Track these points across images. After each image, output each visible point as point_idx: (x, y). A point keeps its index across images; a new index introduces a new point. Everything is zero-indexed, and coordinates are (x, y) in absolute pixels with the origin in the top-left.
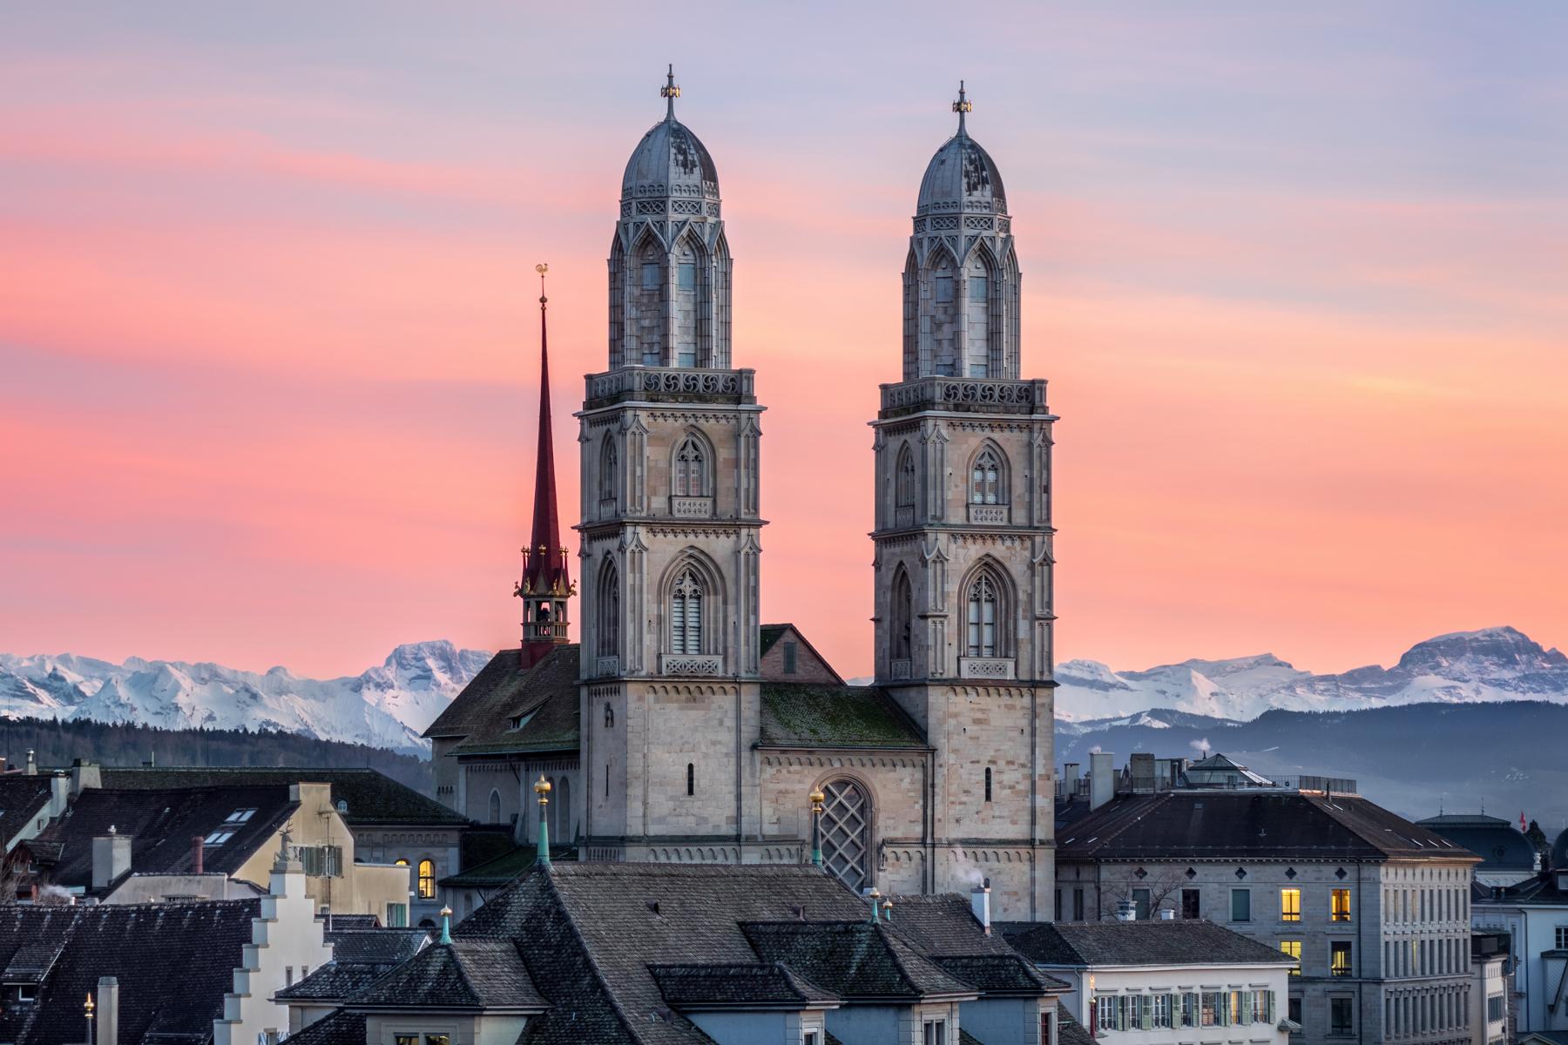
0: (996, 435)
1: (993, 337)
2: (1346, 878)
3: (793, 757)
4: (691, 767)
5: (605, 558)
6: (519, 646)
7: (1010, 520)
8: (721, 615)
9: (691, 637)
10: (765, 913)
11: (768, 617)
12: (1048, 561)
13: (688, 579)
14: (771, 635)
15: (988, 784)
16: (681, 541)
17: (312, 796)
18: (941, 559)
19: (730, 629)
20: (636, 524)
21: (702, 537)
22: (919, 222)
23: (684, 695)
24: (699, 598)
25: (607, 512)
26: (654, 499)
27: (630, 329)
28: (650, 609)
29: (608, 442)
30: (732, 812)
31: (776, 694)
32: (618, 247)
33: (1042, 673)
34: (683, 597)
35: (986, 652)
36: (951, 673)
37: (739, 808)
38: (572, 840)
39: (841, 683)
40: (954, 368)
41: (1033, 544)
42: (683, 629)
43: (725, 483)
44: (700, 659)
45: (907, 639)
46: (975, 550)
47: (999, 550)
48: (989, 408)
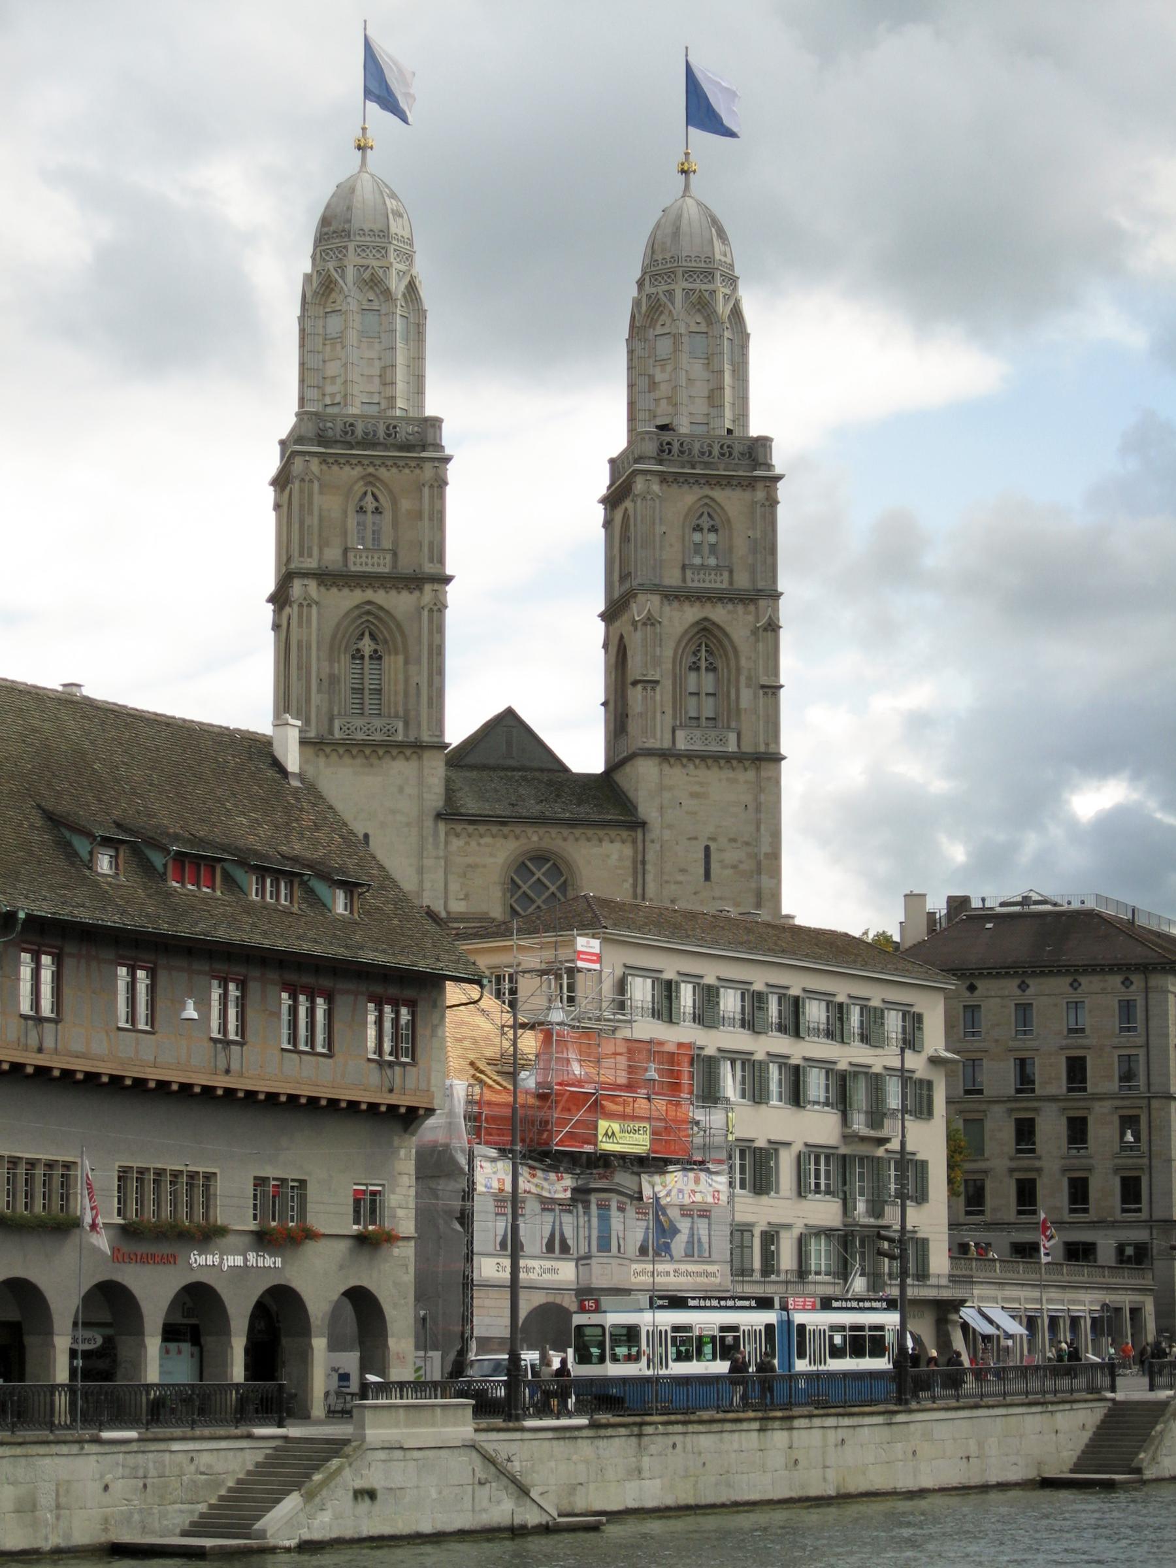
0: (718, 494)
2: (1133, 988)
3: (482, 829)
7: (731, 583)
8: (401, 677)
12: (773, 627)
16: (358, 596)
19: (412, 691)
20: (305, 575)
21: (381, 592)
23: (360, 761)
24: (380, 658)
26: (327, 551)
33: (767, 745)
34: (362, 657)
35: (703, 722)
36: (667, 744)
37: (421, 882)
39: (566, 770)
44: (378, 723)
46: (692, 613)
47: (719, 614)
48: (707, 465)
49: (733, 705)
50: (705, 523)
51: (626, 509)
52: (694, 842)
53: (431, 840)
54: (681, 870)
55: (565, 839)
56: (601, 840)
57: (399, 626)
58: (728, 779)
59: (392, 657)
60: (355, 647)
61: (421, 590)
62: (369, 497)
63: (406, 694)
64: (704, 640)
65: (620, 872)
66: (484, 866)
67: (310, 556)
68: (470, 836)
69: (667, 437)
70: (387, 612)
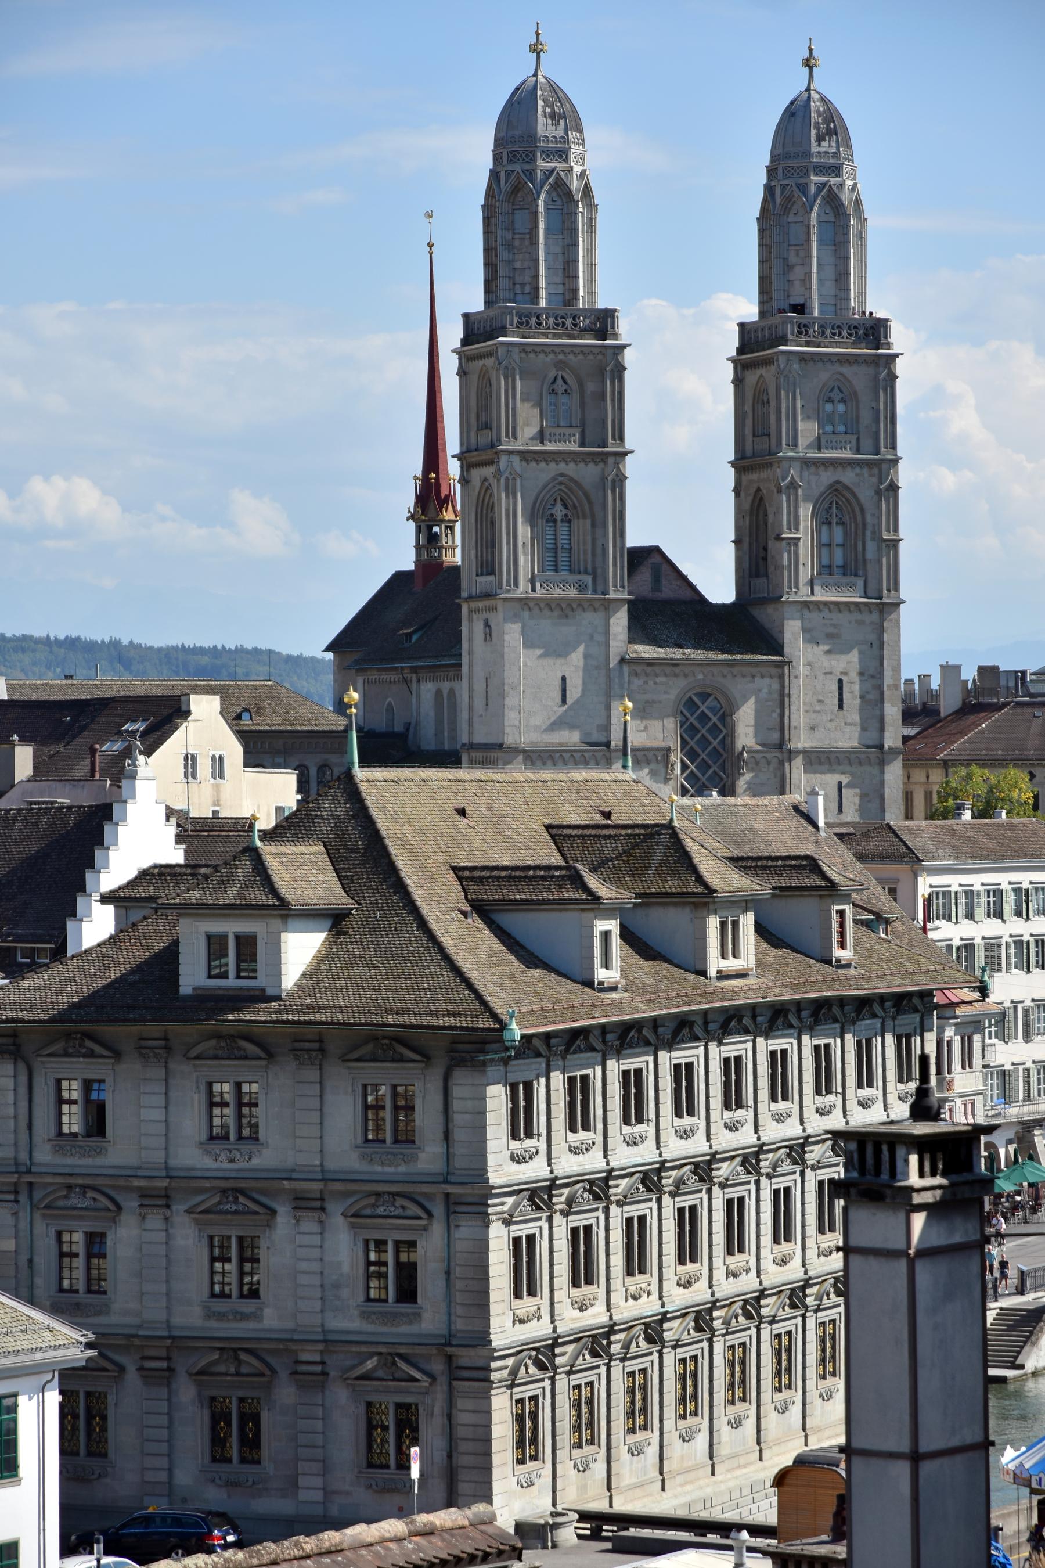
0: (846, 370)
4: (564, 679)
5: (482, 484)
6: (411, 567)
8: (589, 538)
9: (563, 557)
10: (573, 816)
11: (635, 538)
12: (894, 488)
13: (559, 507)
15: (841, 694)
19: (599, 551)
21: (572, 465)
22: (771, 171)
24: (569, 521)
26: (526, 429)
30: (601, 721)
34: (555, 521)
38: (458, 747)
41: (880, 471)
42: (555, 550)
45: (765, 559)
46: (827, 477)
47: (848, 477)
49: (860, 557)
50: (836, 395)
51: (761, 376)
52: (828, 676)
53: (617, 680)
54: (819, 701)
55: (724, 676)
56: (753, 676)
57: (587, 496)
58: (856, 621)
59: (581, 521)
60: (549, 513)
61: (605, 463)
62: (560, 381)
63: (594, 554)
64: (835, 498)
65: (770, 703)
66: (660, 702)
67: (515, 437)
68: (647, 675)
69: (804, 319)
70: (576, 482)
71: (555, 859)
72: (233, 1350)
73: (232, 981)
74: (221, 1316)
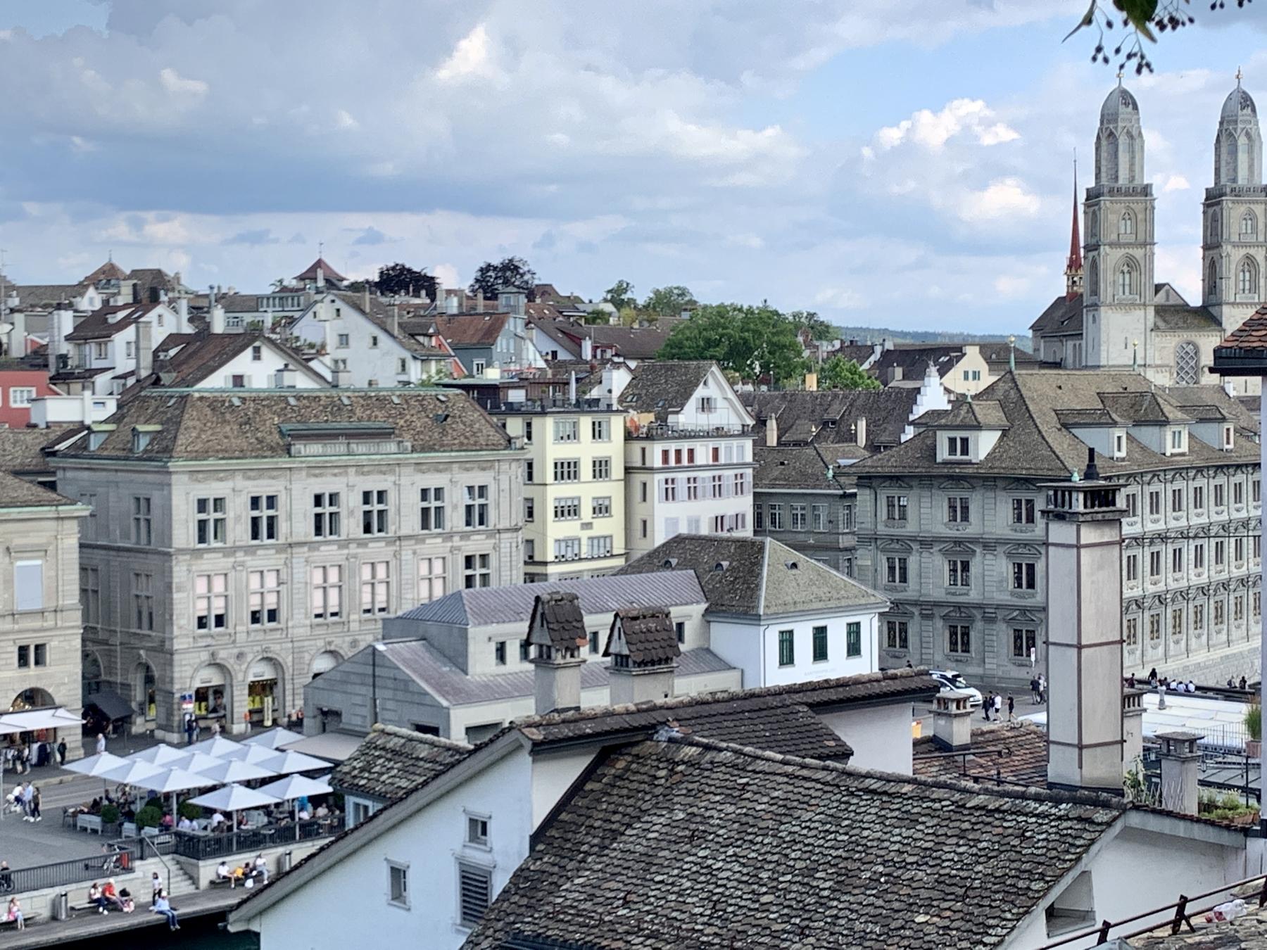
1: (1251, 167)
11: (1156, 282)
14: (1158, 288)
16: (1123, 251)
17: (972, 353)
18: (1228, 255)
22: (1221, 123)
25: (1094, 241)
27: (1103, 169)
28: (1110, 278)
29: (1094, 212)
31: (1161, 311)
32: (1098, 138)
36: (1232, 300)
40: (1234, 180)
43: (1141, 228)
46: (1243, 252)
47: (1252, 251)
71: (1101, 406)
72: (958, 607)
73: (959, 457)
74: (954, 594)
